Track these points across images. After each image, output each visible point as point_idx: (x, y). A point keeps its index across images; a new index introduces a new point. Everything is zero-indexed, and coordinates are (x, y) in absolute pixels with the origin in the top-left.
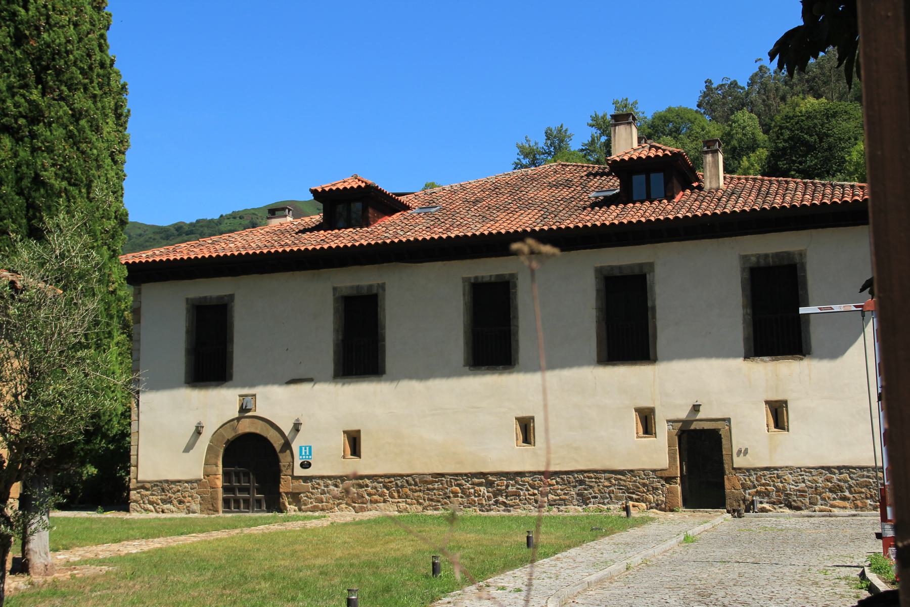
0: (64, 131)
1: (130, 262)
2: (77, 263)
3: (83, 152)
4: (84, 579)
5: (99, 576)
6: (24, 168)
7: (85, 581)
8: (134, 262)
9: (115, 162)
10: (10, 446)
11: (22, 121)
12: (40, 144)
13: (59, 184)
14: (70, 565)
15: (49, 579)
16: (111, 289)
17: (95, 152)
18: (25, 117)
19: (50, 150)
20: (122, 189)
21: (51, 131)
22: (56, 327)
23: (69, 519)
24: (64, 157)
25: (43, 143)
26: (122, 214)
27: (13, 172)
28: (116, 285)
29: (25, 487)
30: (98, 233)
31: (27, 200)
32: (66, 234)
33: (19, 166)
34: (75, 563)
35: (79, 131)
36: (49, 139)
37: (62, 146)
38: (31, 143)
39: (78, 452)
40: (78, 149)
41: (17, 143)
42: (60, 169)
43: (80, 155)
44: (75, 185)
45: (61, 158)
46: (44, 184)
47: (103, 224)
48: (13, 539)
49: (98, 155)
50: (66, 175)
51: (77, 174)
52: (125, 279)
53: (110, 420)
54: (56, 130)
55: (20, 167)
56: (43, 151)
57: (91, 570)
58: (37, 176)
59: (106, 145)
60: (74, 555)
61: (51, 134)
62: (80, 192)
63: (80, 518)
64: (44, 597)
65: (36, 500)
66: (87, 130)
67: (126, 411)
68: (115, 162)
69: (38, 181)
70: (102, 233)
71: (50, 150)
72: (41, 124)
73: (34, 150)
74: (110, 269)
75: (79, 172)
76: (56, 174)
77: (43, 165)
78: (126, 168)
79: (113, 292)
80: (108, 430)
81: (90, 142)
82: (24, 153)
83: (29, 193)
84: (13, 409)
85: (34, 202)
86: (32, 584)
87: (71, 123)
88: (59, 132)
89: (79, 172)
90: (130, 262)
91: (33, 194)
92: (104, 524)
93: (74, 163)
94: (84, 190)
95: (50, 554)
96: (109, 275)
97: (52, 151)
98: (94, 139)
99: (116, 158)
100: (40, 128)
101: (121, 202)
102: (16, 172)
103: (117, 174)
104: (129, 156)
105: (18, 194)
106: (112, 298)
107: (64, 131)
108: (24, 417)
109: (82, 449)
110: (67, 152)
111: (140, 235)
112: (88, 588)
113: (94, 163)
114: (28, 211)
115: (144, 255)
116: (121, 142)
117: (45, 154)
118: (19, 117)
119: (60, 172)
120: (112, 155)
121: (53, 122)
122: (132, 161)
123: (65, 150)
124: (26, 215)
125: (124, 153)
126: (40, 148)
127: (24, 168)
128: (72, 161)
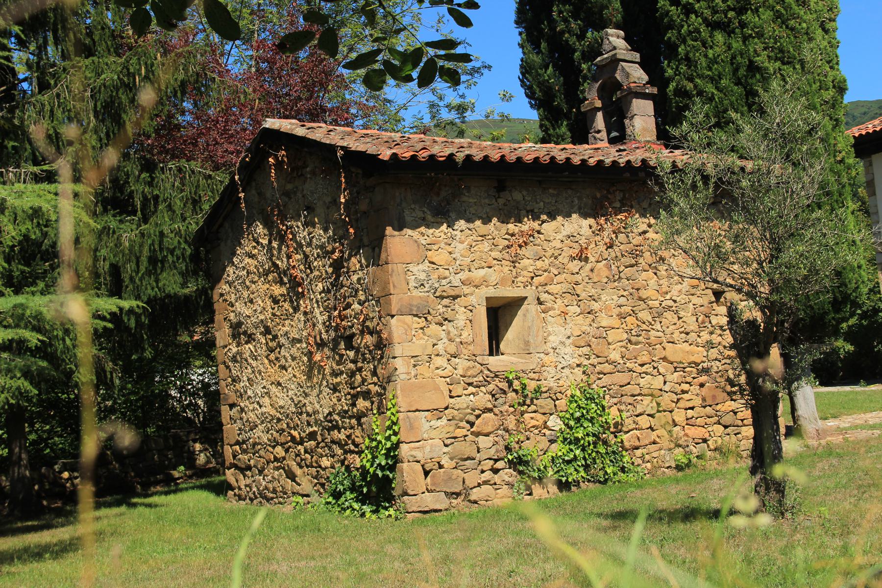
0: (771, 13)
1: (857, 135)
2: (799, 125)
3: (792, 29)
4: (858, 442)
5: (871, 438)
6: (739, 58)
7: (858, 443)
8: (861, 135)
9: (826, 31)
10: (762, 309)
11: (731, 14)
12: (750, 32)
13: (772, 66)
14: (840, 431)
15: (823, 442)
16: (838, 159)
17: (804, 25)
18: (733, 9)
19: (760, 35)
20: (837, 56)
21: (758, 16)
22: (787, 192)
23: (833, 393)
24: (775, 39)
25: (752, 30)
26: (840, 81)
27: (729, 65)
28: (844, 153)
29: (783, 347)
30: (818, 105)
31: (745, 88)
32: (785, 106)
33: (734, 57)
34: (845, 429)
35: (786, 10)
36: (758, 24)
37: (772, 29)
38: (742, 33)
39: (830, 322)
40: (787, 27)
41: (729, 36)
42: (772, 51)
43: (790, 32)
44: (788, 63)
45: (772, 40)
46: (759, 69)
47: (821, 96)
48: (780, 395)
49: (808, 28)
50: (779, 56)
51: (789, 52)
52: (851, 146)
53: (857, 288)
54: (764, 14)
55: (735, 58)
56: (754, 38)
57: (864, 434)
58: (751, 62)
59: (815, 16)
60: (845, 422)
61: (760, 18)
62: (794, 68)
63: (844, 392)
64: (821, 457)
65: (794, 357)
66: (794, 6)
67: (874, 287)
68: (826, 31)
69: (753, 68)
70: (821, 105)
71: (760, 35)
72: (749, 12)
73: (745, 39)
74: (835, 138)
75: (791, 50)
76: (769, 57)
77: (755, 51)
78: (838, 35)
79: (842, 161)
80: (857, 297)
81: (798, 17)
82: (737, 44)
83: (746, 80)
84: (759, 275)
85: (752, 89)
86: (807, 447)
87: (777, 3)
88: (767, 15)
89: (791, 50)
90: (857, 135)
91: (750, 81)
92: (869, 395)
93: (784, 42)
94: (798, 66)
95: (820, 422)
96: (835, 145)
97: (762, 36)
98: (802, 13)
99: (827, 26)
100: (749, 16)
101: (838, 70)
102: (732, 64)
103: (829, 43)
104: (840, 22)
105: (736, 84)
106: (840, 167)
107: (771, 13)
108: (771, 281)
109: (833, 318)
110: (777, 32)
111: (865, 113)
112: (863, 449)
113: (805, 37)
114: (747, 99)
115: (870, 126)
116: (831, 9)
117: (756, 40)
118: (727, 11)
119: (772, 54)
120: (822, 26)
121: (760, 7)
122: (843, 29)
123: (775, 31)
124: (746, 102)
125: (834, 20)
126: (751, 35)
127: (739, 58)
128: (782, 41)
